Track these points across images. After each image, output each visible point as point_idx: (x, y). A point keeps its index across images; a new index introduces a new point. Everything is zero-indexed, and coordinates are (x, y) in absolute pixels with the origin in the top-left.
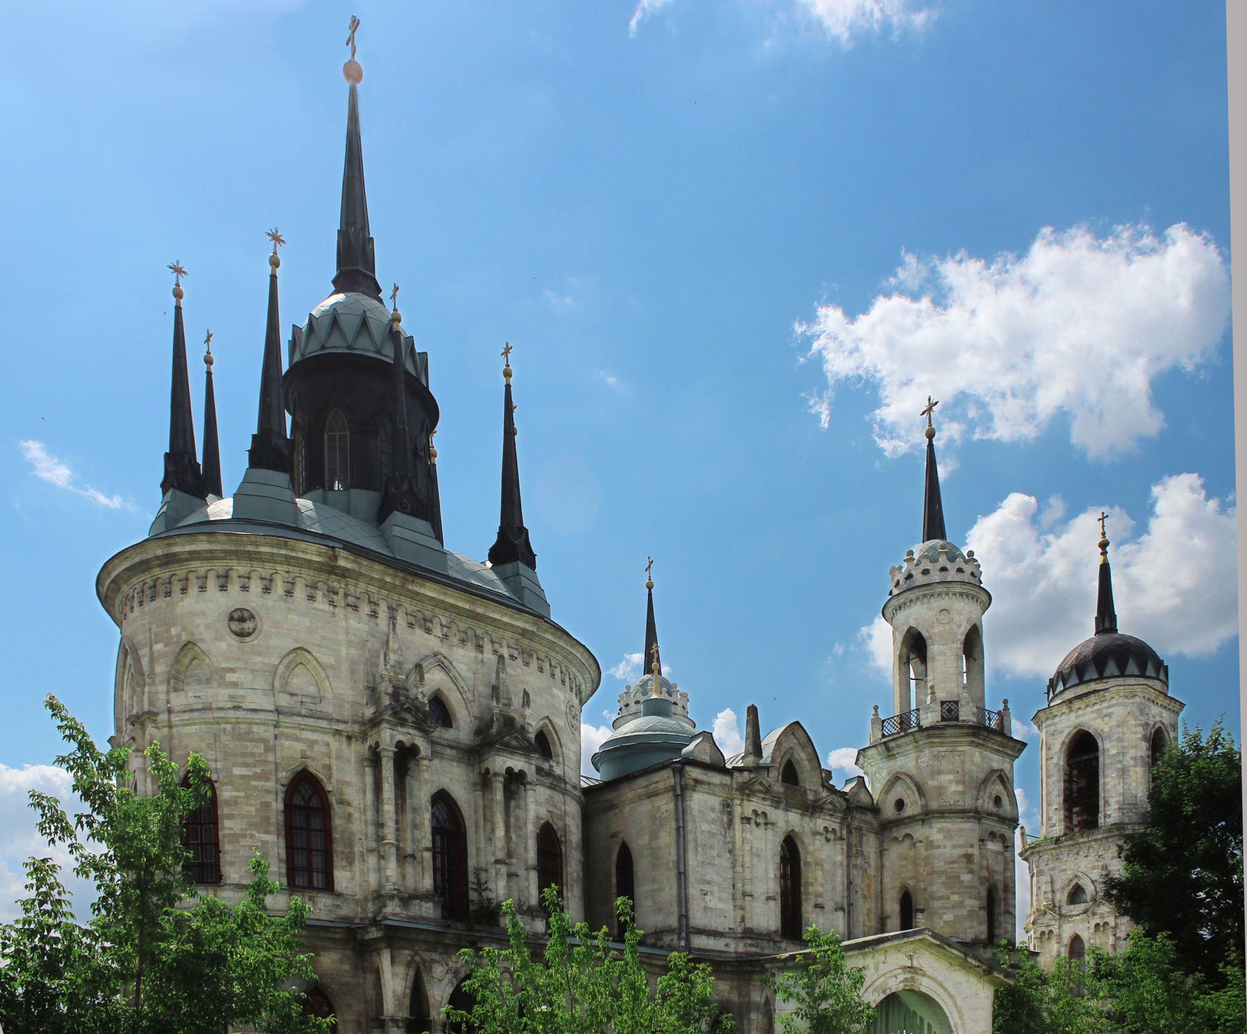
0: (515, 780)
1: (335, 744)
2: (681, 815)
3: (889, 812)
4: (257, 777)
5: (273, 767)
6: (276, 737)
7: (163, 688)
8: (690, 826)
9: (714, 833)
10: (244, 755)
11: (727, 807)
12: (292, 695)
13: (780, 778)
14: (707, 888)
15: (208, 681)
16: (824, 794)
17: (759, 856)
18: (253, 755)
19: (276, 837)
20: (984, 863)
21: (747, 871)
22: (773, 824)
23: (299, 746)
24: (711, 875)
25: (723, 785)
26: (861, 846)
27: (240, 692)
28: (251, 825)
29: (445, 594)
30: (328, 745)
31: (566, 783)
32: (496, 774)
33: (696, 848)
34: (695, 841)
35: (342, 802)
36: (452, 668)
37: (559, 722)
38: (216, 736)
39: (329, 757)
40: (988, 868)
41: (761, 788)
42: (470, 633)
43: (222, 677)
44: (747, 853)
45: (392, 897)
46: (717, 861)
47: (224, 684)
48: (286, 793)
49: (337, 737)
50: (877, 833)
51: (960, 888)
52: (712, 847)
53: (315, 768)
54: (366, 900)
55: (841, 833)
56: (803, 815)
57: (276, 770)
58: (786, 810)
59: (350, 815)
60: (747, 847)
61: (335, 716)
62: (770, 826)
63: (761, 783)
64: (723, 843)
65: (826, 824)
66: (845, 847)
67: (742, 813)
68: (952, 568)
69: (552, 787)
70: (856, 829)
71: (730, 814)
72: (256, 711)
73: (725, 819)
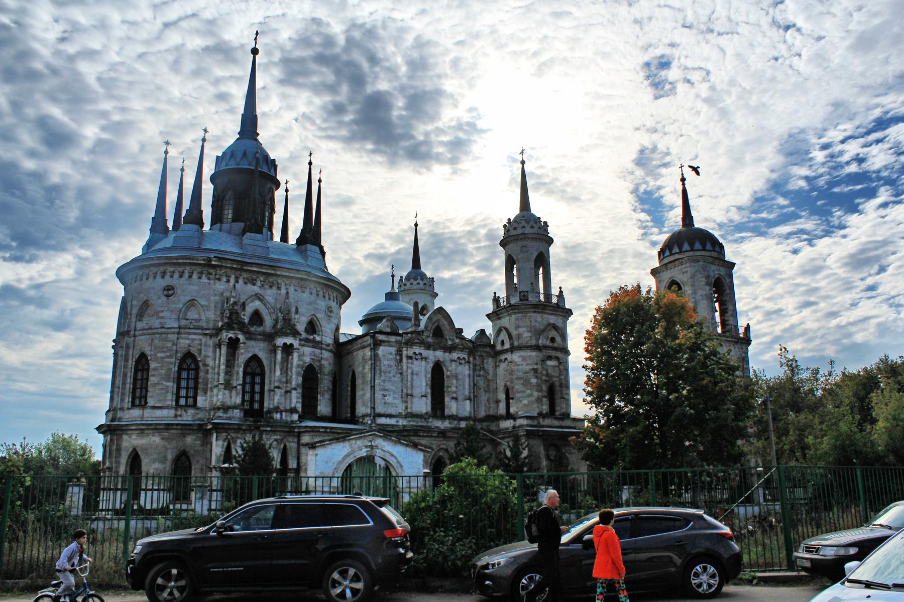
0: (288, 349)
1: (204, 340)
2: (375, 358)
3: (499, 347)
4: (167, 357)
5: (174, 352)
6: (178, 339)
7: (134, 320)
8: (378, 364)
10: (162, 348)
11: (399, 352)
12: (187, 319)
15: (153, 316)
16: (457, 341)
18: (167, 347)
20: (545, 372)
21: (409, 383)
23: (188, 342)
24: (388, 386)
25: (397, 342)
27: (166, 321)
28: (162, 379)
30: (201, 340)
31: (322, 344)
32: (278, 347)
33: (380, 374)
34: (380, 370)
35: (205, 365)
37: (319, 316)
38: (152, 340)
39: (201, 345)
40: (547, 375)
43: (158, 315)
45: (219, 409)
47: (158, 317)
48: (179, 363)
50: (493, 357)
52: (390, 372)
53: (194, 351)
54: (211, 410)
56: (444, 352)
57: (176, 353)
58: (434, 350)
59: (208, 371)
60: (409, 371)
61: (205, 327)
65: (459, 355)
66: (471, 366)
70: (479, 356)
71: (401, 355)
72: (170, 328)
73: (398, 358)
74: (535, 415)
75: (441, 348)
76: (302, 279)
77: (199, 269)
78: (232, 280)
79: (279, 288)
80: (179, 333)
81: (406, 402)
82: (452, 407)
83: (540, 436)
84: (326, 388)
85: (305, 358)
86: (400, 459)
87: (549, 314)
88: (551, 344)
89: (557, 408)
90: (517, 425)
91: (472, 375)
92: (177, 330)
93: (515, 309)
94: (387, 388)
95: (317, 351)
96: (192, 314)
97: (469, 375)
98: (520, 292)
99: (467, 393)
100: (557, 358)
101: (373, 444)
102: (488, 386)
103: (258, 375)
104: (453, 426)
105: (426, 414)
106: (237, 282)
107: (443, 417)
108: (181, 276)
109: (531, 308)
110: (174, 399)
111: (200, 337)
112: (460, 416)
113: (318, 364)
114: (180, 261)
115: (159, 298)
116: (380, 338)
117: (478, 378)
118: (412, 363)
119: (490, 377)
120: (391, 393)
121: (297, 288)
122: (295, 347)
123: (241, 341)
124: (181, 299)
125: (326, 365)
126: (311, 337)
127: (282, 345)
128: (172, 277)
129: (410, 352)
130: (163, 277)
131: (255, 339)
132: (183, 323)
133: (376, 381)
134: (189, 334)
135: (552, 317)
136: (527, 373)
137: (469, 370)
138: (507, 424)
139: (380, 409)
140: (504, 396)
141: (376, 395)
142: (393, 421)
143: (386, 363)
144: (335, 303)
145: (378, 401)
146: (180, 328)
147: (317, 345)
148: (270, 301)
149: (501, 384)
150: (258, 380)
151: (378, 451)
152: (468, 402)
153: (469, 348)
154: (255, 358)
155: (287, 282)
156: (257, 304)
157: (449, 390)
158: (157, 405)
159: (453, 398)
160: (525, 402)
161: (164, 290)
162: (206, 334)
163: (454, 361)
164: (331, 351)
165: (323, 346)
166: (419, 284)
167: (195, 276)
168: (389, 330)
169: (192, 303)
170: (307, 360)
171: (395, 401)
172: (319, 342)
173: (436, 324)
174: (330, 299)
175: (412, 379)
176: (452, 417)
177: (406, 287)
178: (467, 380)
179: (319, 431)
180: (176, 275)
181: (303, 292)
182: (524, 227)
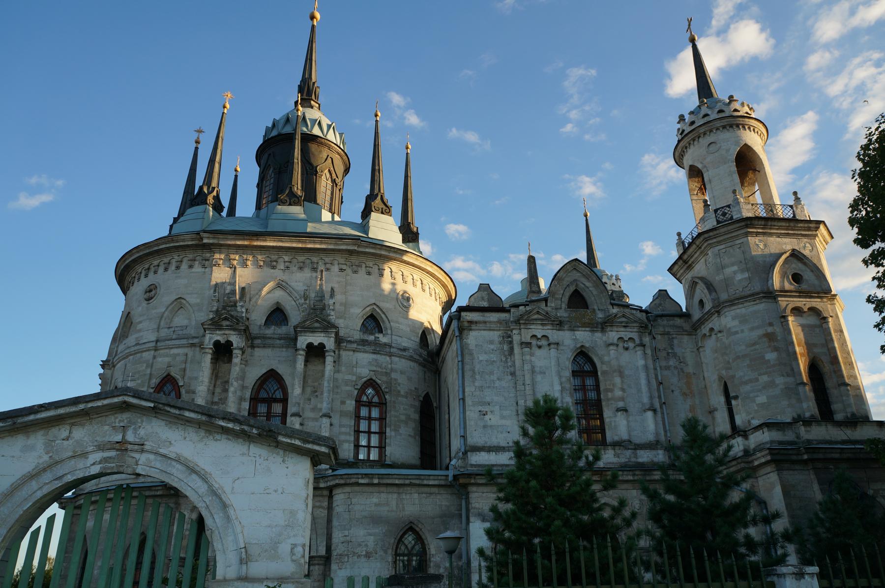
0: (316, 353)
1: (190, 354)
3: (697, 315)
5: (148, 377)
6: (154, 357)
8: (467, 359)
9: (494, 361)
11: (507, 338)
13: (564, 306)
16: (615, 310)
22: (558, 344)
23: (167, 359)
25: (500, 322)
26: (672, 349)
30: (187, 355)
34: (473, 371)
36: (288, 286)
41: (540, 317)
42: (308, 261)
44: (526, 372)
46: (497, 384)
49: (193, 348)
50: (690, 334)
52: (492, 373)
55: (641, 340)
56: (590, 331)
57: (150, 379)
58: (572, 329)
61: (194, 335)
62: (552, 346)
63: (538, 313)
64: (504, 367)
65: (622, 334)
66: (649, 352)
67: (521, 339)
71: (511, 342)
73: (506, 347)
75: (584, 325)
76: (351, 252)
77: (191, 256)
80: (156, 350)
83: (805, 462)
84: (403, 417)
85: (359, 370)
86: (221, 481)
89: (835, 407)
90: (752, 446)
91: (651, 366)
92: (153, 344)
93: (710, 238)
94: (488, 399)
95: (383, 359)
96: (180, 320)
97: (646, 367)
98: (716, 211)
99: (646, 400)
100: (813, 310)
101: (130, 437)
103: (276, 400)
104: (623, 460)
109: (741, 228)
111: (186, 350)
112: (637, 441)
113: (384, 378)
114: (161, 247)
115: (139, 306)
116: (469, 318)
117: (666, 373)
118: (532, 355)
119: (690, 369)
120: (497, 407)
121: (344, 267)
122: (327, 348)
123: (235, 345)
124: (164, 299)
125: (400, 381)
126: (372, 338)
127: (304, 347)
128: (155, 272)
129: (526, 336)
130: (146, 276)
131: (273, 346)
132: (164, 333)
133: (467, 390)
136: (754, 344)
137: (645, 358)
139: (476, 437)
140: (722, 399)
141: (468, 413)
143: (483, 357)
145: (470, 423)
146: (157, 341)
147: (379, 348)
148: (297, 288)
149: (711, 376)
150: (277, 408)
151: (143, 458)
152: (650, 414)
153: (641, 322)
154: (272, 376)
155: (327, 260)
157: (610, 395)
159: (618, 410)
160: (762, 399)
161: (146, 292)
162: (193, 345)
164: (411, 358)
165: (392, 350)
167: (184, 266)
168: (485, 304)
169: (179, 303)
170: (365, 373)
171: (507, 422)
172: (385, 344)
173: (572, 289)
175: (533, 380)
176: (618, 444)
178: (643, 376)
179: (358, 484)
180: (161, 270)
181: (355, 272)
182: (706, 115)
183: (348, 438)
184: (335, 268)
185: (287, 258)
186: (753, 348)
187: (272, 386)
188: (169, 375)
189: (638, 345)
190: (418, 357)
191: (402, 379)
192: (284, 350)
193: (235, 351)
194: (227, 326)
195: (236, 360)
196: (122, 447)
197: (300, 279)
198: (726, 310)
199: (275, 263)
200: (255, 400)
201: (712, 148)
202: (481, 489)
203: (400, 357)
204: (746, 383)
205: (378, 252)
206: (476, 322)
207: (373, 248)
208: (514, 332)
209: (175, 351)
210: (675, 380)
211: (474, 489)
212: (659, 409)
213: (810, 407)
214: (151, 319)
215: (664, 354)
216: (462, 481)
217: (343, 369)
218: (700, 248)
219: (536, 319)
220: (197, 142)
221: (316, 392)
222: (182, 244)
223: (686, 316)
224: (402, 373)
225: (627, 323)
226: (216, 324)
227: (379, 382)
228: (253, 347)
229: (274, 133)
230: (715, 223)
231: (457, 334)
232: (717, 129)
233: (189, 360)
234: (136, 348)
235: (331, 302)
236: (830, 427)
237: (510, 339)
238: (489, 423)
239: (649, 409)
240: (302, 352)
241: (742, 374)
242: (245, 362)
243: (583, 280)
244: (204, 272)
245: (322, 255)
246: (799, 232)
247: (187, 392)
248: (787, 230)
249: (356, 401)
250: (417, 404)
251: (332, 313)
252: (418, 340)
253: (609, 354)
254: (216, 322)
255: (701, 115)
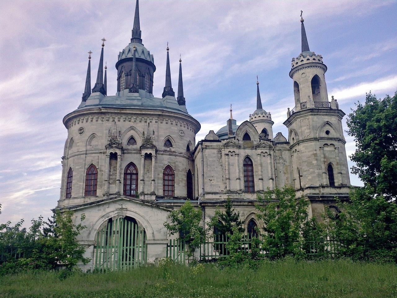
3: (292, 143)
4: (81, 168)
6: (86, 157)
11: (220, 151)
14: (211, 178)
17: (233, 165)
19: (82, 183)
25: (217, 146)
26: (282, 156)
29: (133, 111)
34: (207, 164)
44: (226, 165)
51: (313, 166)
52: (214, 165)
55: (270, 152)
57: (85, 166)
58: (244, 148)
60: (227, 163)
62: (236, 155)
65: (262, 151)
66: (272, 157)
68: (311, 59)
69: (170, 155)
71: (221, 153)
73: (219, 155)
74: (318, 186)
76: (159, 115)
77: (97, 116)
78: (116, 120)
79: (146, 122)
81: (225, 183)
82: (259, 185)
84: (181, 179)
87: (323, 115)
88: (326, 136)
89: (335, 181)
90: (305, 194)
91: (273, 163)
92: (85, 152)
94: (212, 175)
95: (173, 157)
97: (271, 163)
99: (270, 175)
102: (287, 170)
105: (240, 190)
106: (119, 121)
107: (253, 192)
108: (87, 121)
110: (84, 192)
111: (99, 155)
114: (84, 112)
117: (279, 165)
120: (215, 178)
121: (157, 121)
122: (153, 155)
123: (118, 154)
126: (168, 149)
127: (144, 155)
128: (82, 122)
129: (226, 151)
130: (78, 123)
132: (89, 147)
134: (92, 153)
135: (326, 117)
136: (309, 157)
138: (299, 194)
139: (208, 189)
142: (217, 197)
144: (186, 128)
146: (86, 151)
147: (172, 153)
149: (295, 167)
150: (134, 177)
152: (271, 181)
154: (132, 164)
155: (151, 118)
156: (132, 133)
158: (75, 196)
159: (260, 179)
160: (310, 177)
162: (101, 153)
163: (259, 155)
165: (176, 154)
166: (260, 117)
167: (94, 120)
168: (212, 139)
169: (93, 136)
170: (166, 163)
174: (181, 126)
177: (253, 120)
178: (269, 166)
181: (162, 123)
182: (302, 61)
183: (161, 188)
184: (154, 121)
185: (135, 117)
186: (309, 158)
187: (132, 168)
188: (92, 164)
189: (269, 155)
190: (185, 156)
191: (180, 165)
192: (136, 154)
193: (118, 157)
194: (115, 147)
195: (119, 160)
196: (122, 209)
197: (141, 126)
198: (301, 143)
199: (130, 119)
200: (126, 174)
201: (304, 75)
202: (209, 207)
203: (181, 156)
204: (305, 171)
205: (170, 115)
206: (208, 146)
207: (168, 113)
208: (222, 149)
209: (94, 155)
210: (281, 168)
211: (207, 207)
212: (274, 179)
213: (325, 181)
214: (83, 142)
215: (278, 158)
216: (202, 205)
217: (158, 162)
218: (294, 118)
219: (230, 145)
220: (90, 58)
221: (148, 170)
222: (93, 112)
223: (287, 143)
224: (180, 162)
225: (265, 146)
226: (110, 146)
227: (172, 166)
228: (124, 153)
229: (124, 57)
230: (300, 109)
231: (201, 150)
232: (306, 67)
233: (100, 158)
234: (78, 153)
235: (153, 136)
236: (331, 189)
237: (221, 152)
238: (213, 184)
239: (271, 179)
240: (143, 157)
241: (304, 168)
242: (122, 160)
243: (249, 129)
244: (102, 123)
245: (149, 116)
246: (331, 114)
247: (100, 171)
248: (327, 113)
249: (163, 174)
250: (186, 174)
251: (154, 141)
252: (186, 149)
253: (257, 158)
254: (111, 145)
255: (300, 61)
